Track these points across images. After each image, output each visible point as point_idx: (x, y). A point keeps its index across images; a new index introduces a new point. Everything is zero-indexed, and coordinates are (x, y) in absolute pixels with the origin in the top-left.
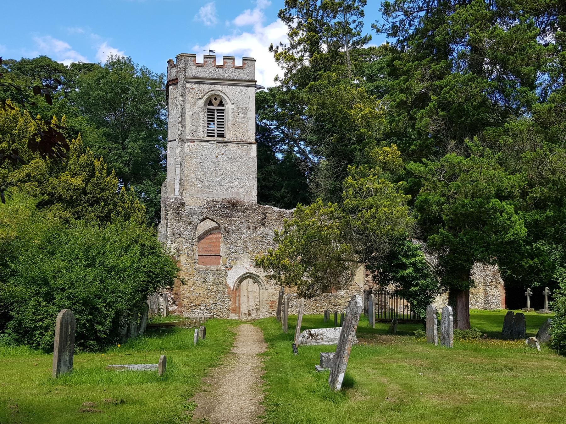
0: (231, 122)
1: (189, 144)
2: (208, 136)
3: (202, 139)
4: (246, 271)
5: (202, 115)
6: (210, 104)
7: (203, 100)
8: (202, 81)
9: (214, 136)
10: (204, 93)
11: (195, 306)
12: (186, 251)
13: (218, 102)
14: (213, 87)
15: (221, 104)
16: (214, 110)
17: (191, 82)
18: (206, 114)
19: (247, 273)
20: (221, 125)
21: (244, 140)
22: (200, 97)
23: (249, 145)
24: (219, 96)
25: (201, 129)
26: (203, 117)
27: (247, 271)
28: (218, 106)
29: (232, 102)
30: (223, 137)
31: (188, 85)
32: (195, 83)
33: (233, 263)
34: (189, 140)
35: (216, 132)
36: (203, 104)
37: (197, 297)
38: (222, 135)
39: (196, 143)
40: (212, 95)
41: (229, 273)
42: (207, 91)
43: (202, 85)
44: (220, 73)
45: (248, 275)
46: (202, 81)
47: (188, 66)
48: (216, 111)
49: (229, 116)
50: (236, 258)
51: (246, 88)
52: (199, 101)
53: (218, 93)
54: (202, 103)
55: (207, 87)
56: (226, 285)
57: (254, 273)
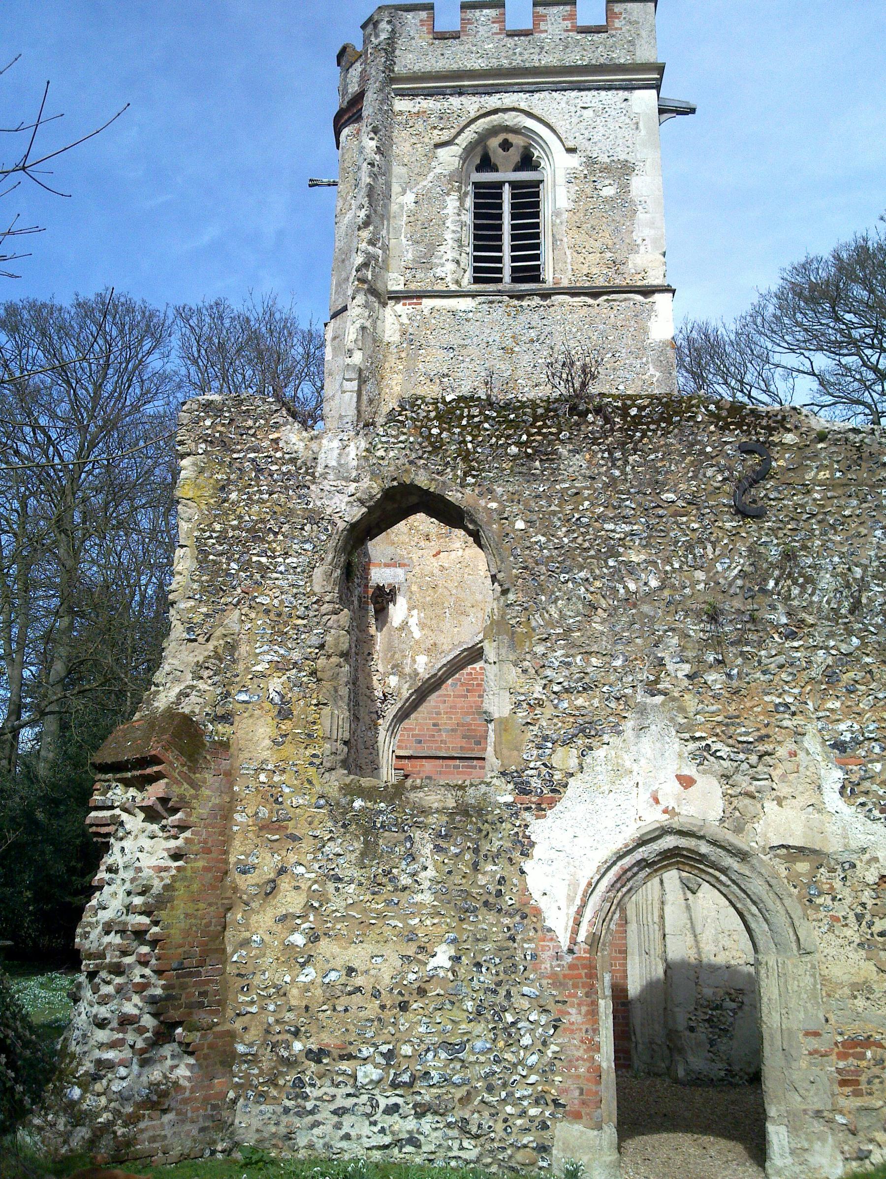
0: (565, 215)
1: (400, 308)
2: (477, 280)
3: (453, 287)
4: (654, 818)
5: (452, 202)
6: (486, 164)
7: (456, 150)
8: (455, 82)
9: (500, 280)
10: (463, 121)
11: (316, 1056)
12: (275, 684)
13: (514, 156)
14: (493, 102)
15: (527, 162)
16: (500, 185)
17: (412, 94)
18: (469, 202)
19: (664, 831)
20: (528, 237)
21: (619, 281)
22: (446, 136)
23: (639, 298)
24: (515, 130)
25: (448, 251)
26: (456, 215)
27: (663, 819)
28: (517, 169)
29: (570, 144)
30: (536, 279)
31: (401, 105)
32: (429, 94)
33: (565, 758)
34: (397, 297)
35: (507, 265)
36: (456, 163)
37: (331, 993)
38: (528, 273)
39: (428, 303)
40: (494, 131)
41: (543, 830)
42: (473, 115)
43: (455, 101)
44: (527, 55)
45: (669, 842)
46: (455, 82)
47: (401, 43)
48: (507, 188)
49: (557, 199)
50: (586, 732)
51: (622, 94)
52: (441, 152)
53: (510, 119)
54: (449, 158)
55: (472, 105)
56: (527, 913)
57: (714, 829)
